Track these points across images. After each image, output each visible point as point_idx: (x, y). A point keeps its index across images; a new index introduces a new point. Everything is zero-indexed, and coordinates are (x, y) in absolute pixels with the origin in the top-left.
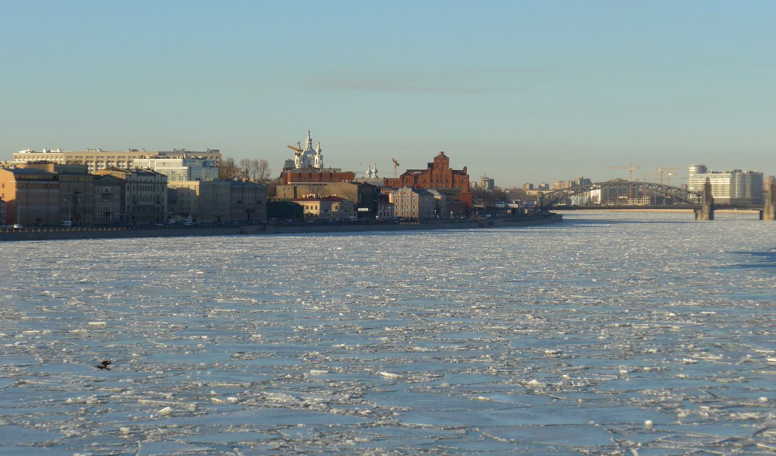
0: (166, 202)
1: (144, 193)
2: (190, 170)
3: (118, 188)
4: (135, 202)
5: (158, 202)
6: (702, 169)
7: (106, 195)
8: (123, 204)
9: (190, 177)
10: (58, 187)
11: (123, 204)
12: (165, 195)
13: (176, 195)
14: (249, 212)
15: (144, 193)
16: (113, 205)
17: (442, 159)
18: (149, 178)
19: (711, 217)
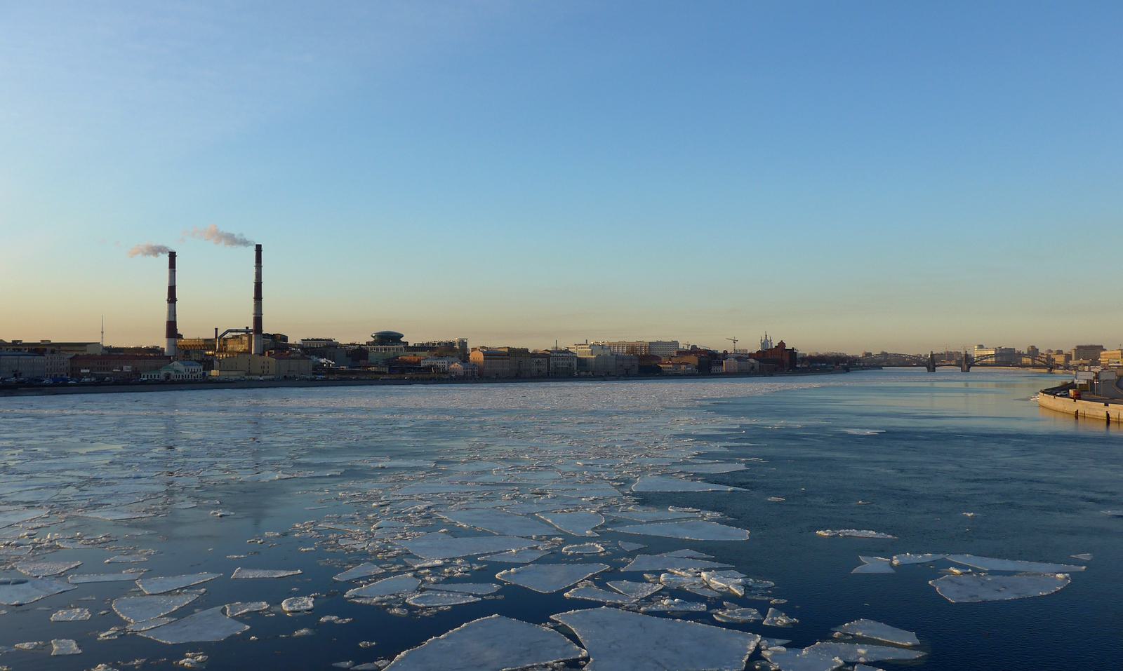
0: (575, 365)
1: (561, 362)
2: (592, 351)
3: (545, 359)
4: (555, 366)
5: (570, 366)
6: (981, 347)
7: (538, 363)
8: (549, 367)
9: (592, 355)
10: (509, 359)
11: (549, 367)
12: (575, 362)
13: (582, 362)
14: (627, 370)
15: (561, 362)
16: (544, 368)
17: (782, 344)
18: (565, 355)
19: (934, 371)
